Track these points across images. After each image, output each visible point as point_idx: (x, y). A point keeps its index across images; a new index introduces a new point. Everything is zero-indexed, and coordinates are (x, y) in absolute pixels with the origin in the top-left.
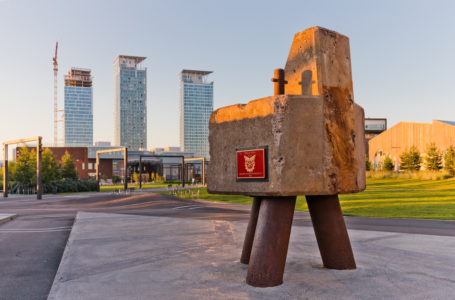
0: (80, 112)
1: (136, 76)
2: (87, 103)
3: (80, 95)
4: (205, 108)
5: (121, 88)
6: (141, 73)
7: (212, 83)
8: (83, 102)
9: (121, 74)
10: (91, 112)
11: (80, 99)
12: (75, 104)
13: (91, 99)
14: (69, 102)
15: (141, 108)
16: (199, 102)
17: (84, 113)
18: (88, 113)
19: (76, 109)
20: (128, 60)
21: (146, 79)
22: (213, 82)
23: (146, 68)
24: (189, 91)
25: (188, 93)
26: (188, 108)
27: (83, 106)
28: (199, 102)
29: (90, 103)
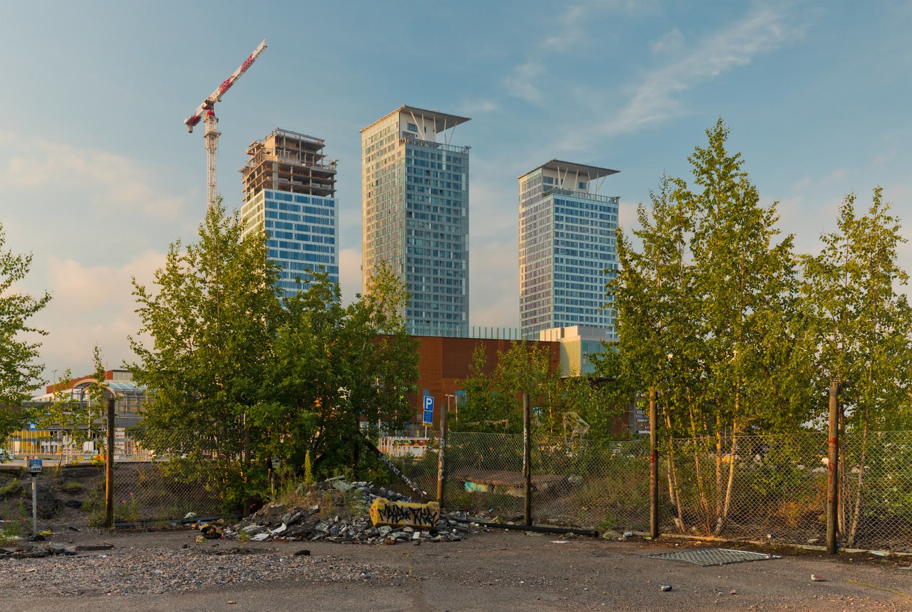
0: (308, 257)
1: (444, 168)
2: (323, 231)
3: (307, 210)
4: (601, 264)
5: (409, 196)
6: (455, 159)
7: (615, 200)
8: (315, 229)
9: (408, 160)
10: (333, 258)
11: (307, 219)
12: (294, 232)
13: (333, 222)
14: (278, 225)
15: (454, 254)
16: (587, 246)
17: (315, 258)
18: (326, 259)
19: (296, 246)
20: (420, 125)
21: (467, 177)
22: (618, 198)
23: (467, 148)
24: (564, 215)
25: (564, 223)
26: (562, 260)
27: (315, 239)
28: (587, 246)
29: (332, 231)
